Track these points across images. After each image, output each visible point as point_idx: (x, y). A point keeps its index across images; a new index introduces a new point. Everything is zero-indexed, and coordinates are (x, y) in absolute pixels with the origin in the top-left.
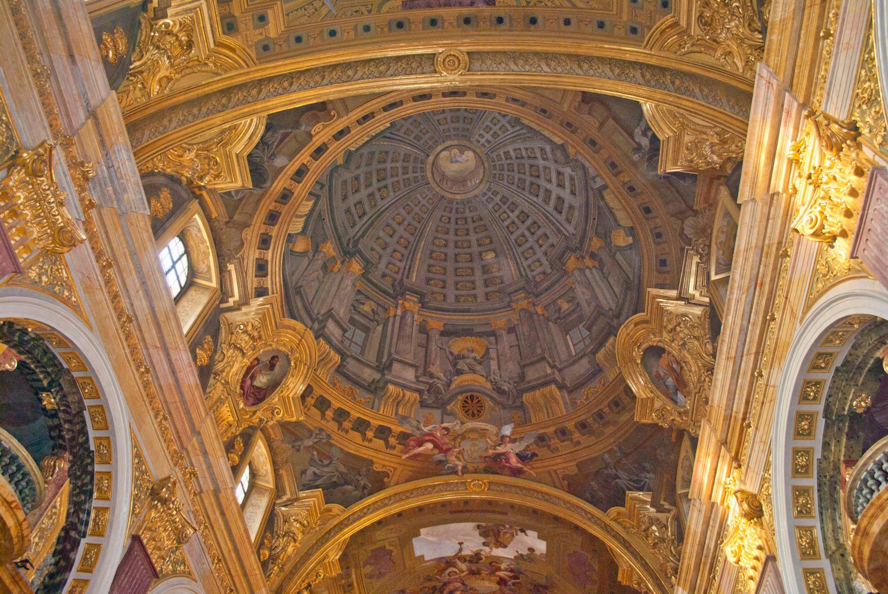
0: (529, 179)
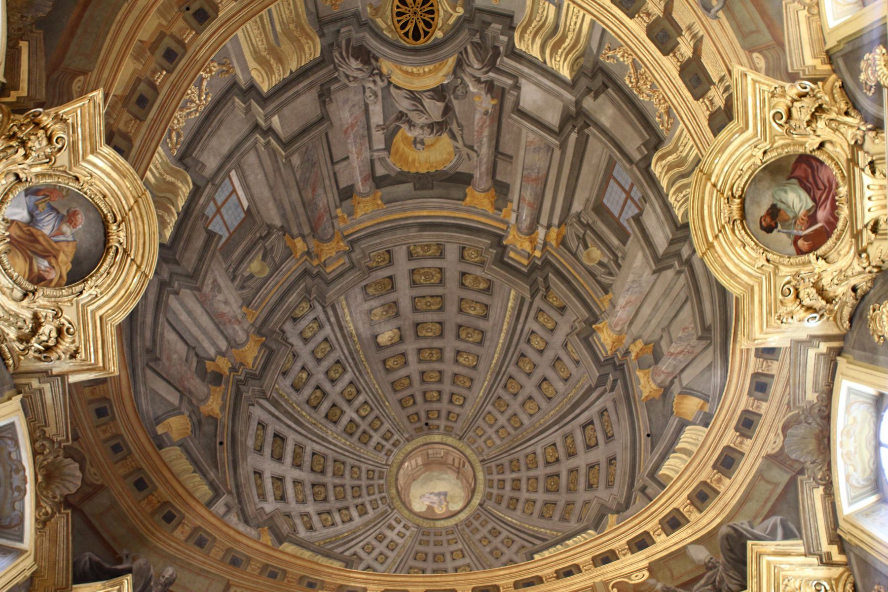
0: (329, 479)
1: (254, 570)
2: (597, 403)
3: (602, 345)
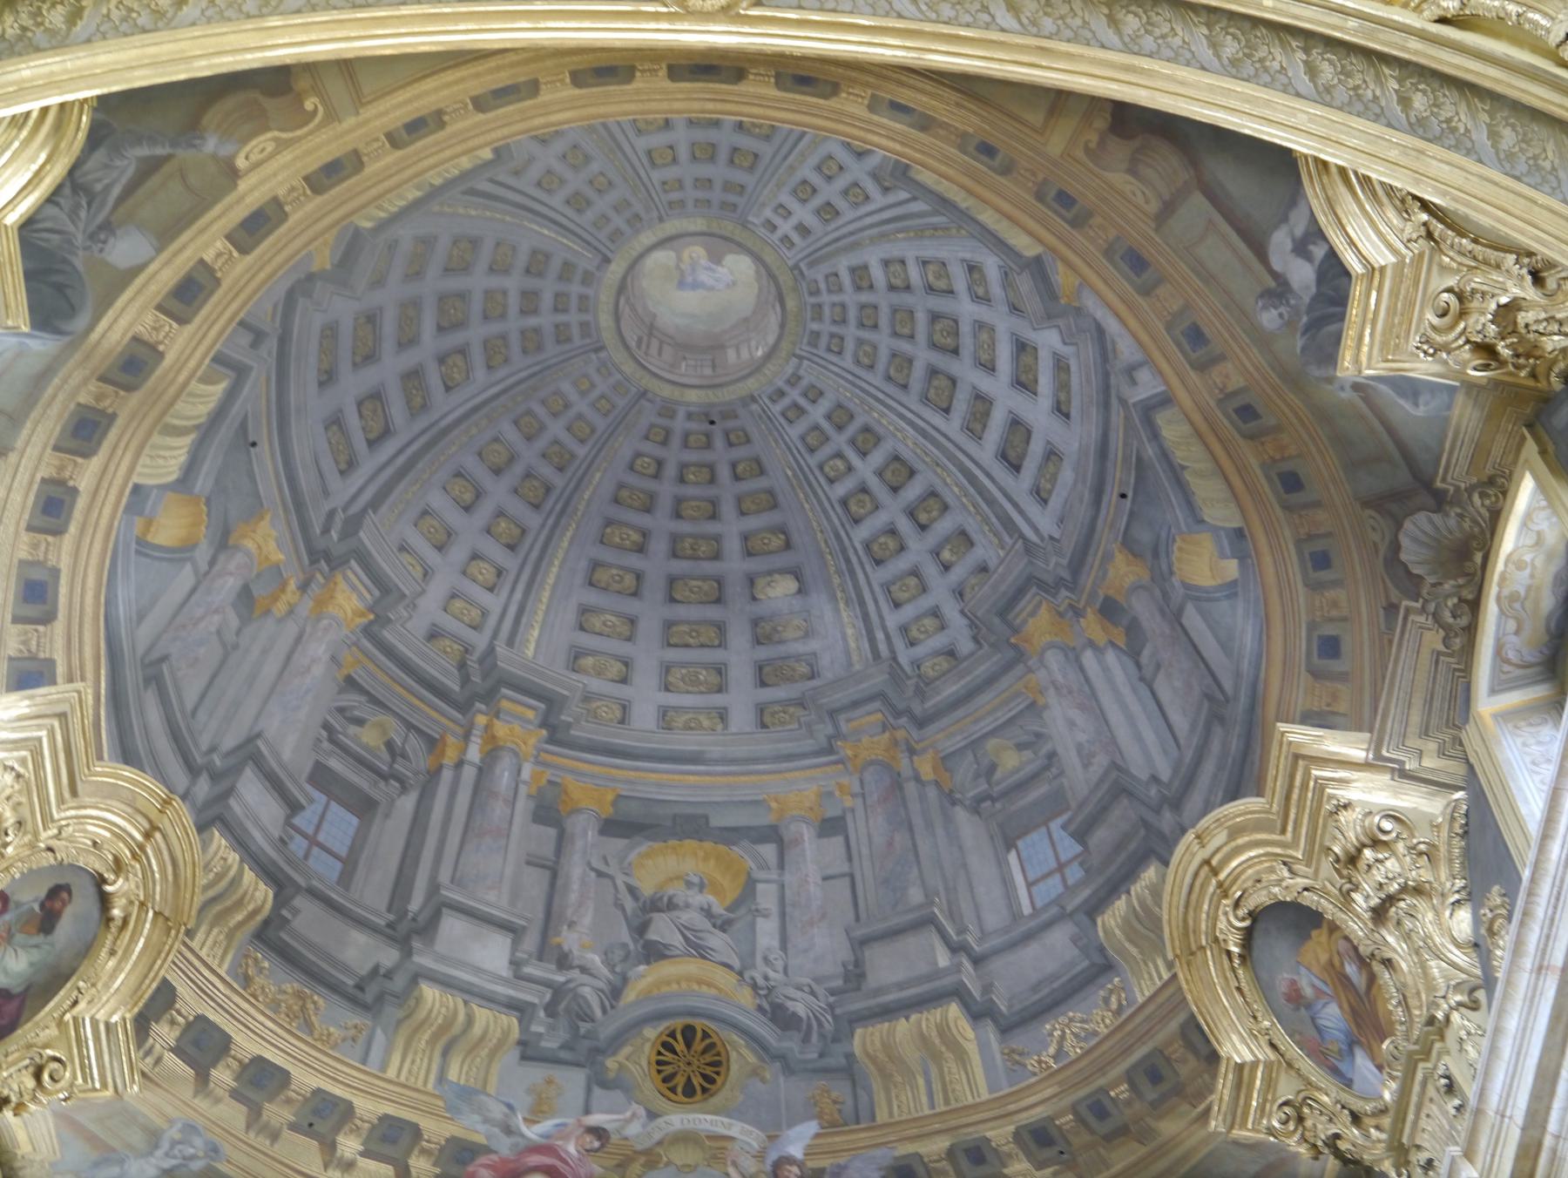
2: (361, 482)
3: (354, 588)
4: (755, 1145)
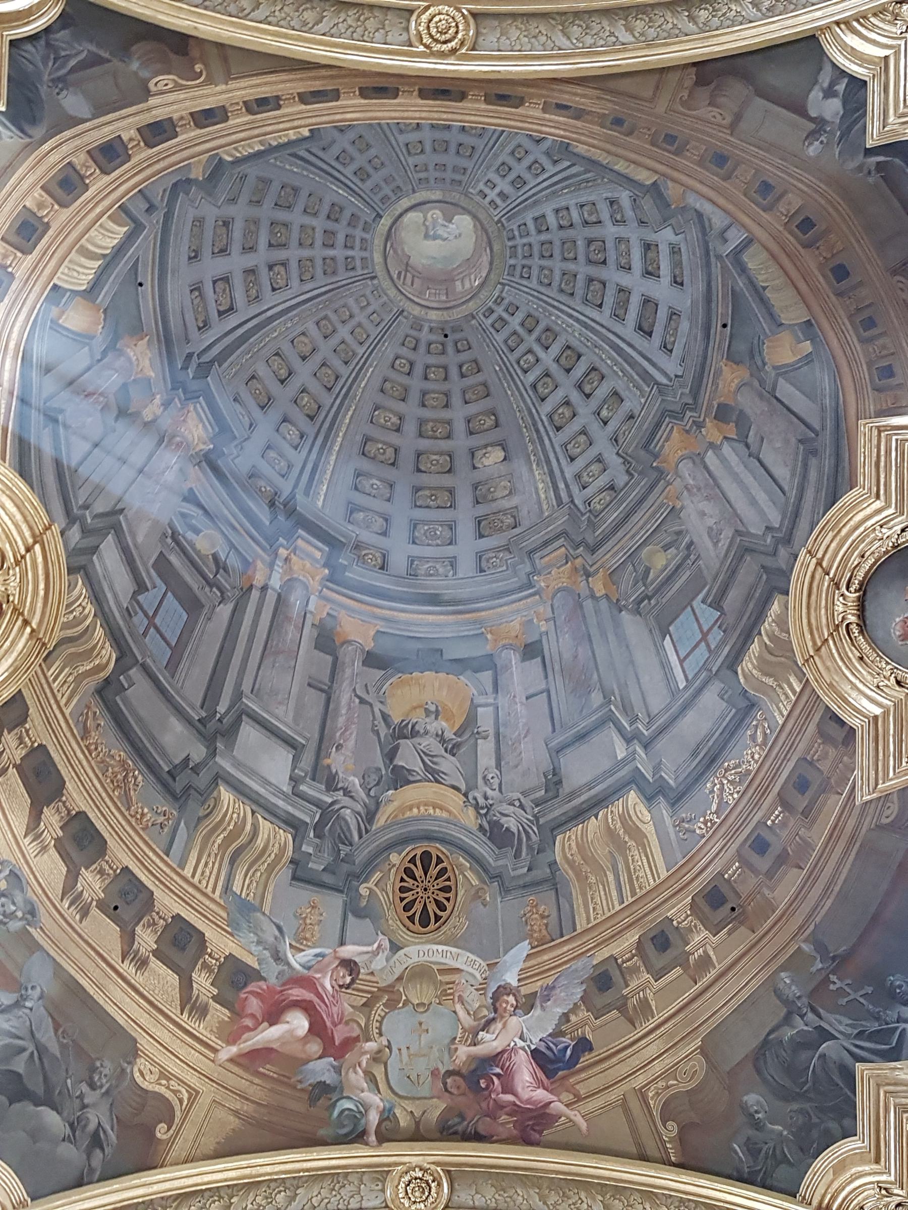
1: (696, 148)
3: (201, 420)
4: (478, 976)
